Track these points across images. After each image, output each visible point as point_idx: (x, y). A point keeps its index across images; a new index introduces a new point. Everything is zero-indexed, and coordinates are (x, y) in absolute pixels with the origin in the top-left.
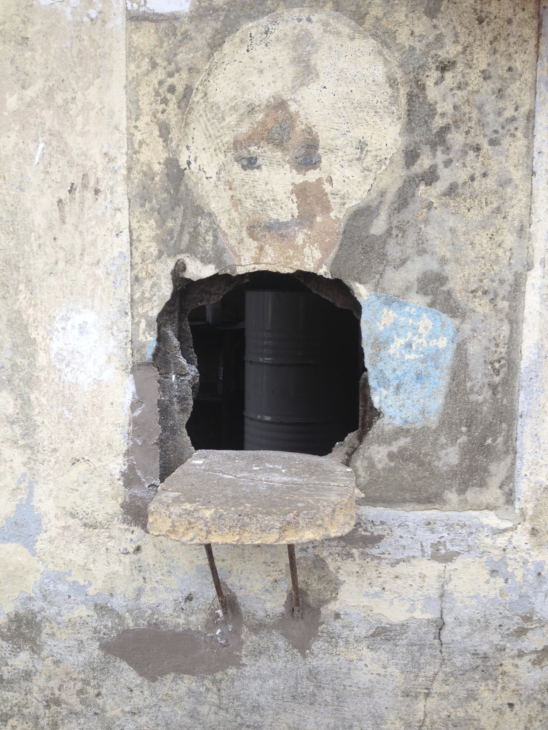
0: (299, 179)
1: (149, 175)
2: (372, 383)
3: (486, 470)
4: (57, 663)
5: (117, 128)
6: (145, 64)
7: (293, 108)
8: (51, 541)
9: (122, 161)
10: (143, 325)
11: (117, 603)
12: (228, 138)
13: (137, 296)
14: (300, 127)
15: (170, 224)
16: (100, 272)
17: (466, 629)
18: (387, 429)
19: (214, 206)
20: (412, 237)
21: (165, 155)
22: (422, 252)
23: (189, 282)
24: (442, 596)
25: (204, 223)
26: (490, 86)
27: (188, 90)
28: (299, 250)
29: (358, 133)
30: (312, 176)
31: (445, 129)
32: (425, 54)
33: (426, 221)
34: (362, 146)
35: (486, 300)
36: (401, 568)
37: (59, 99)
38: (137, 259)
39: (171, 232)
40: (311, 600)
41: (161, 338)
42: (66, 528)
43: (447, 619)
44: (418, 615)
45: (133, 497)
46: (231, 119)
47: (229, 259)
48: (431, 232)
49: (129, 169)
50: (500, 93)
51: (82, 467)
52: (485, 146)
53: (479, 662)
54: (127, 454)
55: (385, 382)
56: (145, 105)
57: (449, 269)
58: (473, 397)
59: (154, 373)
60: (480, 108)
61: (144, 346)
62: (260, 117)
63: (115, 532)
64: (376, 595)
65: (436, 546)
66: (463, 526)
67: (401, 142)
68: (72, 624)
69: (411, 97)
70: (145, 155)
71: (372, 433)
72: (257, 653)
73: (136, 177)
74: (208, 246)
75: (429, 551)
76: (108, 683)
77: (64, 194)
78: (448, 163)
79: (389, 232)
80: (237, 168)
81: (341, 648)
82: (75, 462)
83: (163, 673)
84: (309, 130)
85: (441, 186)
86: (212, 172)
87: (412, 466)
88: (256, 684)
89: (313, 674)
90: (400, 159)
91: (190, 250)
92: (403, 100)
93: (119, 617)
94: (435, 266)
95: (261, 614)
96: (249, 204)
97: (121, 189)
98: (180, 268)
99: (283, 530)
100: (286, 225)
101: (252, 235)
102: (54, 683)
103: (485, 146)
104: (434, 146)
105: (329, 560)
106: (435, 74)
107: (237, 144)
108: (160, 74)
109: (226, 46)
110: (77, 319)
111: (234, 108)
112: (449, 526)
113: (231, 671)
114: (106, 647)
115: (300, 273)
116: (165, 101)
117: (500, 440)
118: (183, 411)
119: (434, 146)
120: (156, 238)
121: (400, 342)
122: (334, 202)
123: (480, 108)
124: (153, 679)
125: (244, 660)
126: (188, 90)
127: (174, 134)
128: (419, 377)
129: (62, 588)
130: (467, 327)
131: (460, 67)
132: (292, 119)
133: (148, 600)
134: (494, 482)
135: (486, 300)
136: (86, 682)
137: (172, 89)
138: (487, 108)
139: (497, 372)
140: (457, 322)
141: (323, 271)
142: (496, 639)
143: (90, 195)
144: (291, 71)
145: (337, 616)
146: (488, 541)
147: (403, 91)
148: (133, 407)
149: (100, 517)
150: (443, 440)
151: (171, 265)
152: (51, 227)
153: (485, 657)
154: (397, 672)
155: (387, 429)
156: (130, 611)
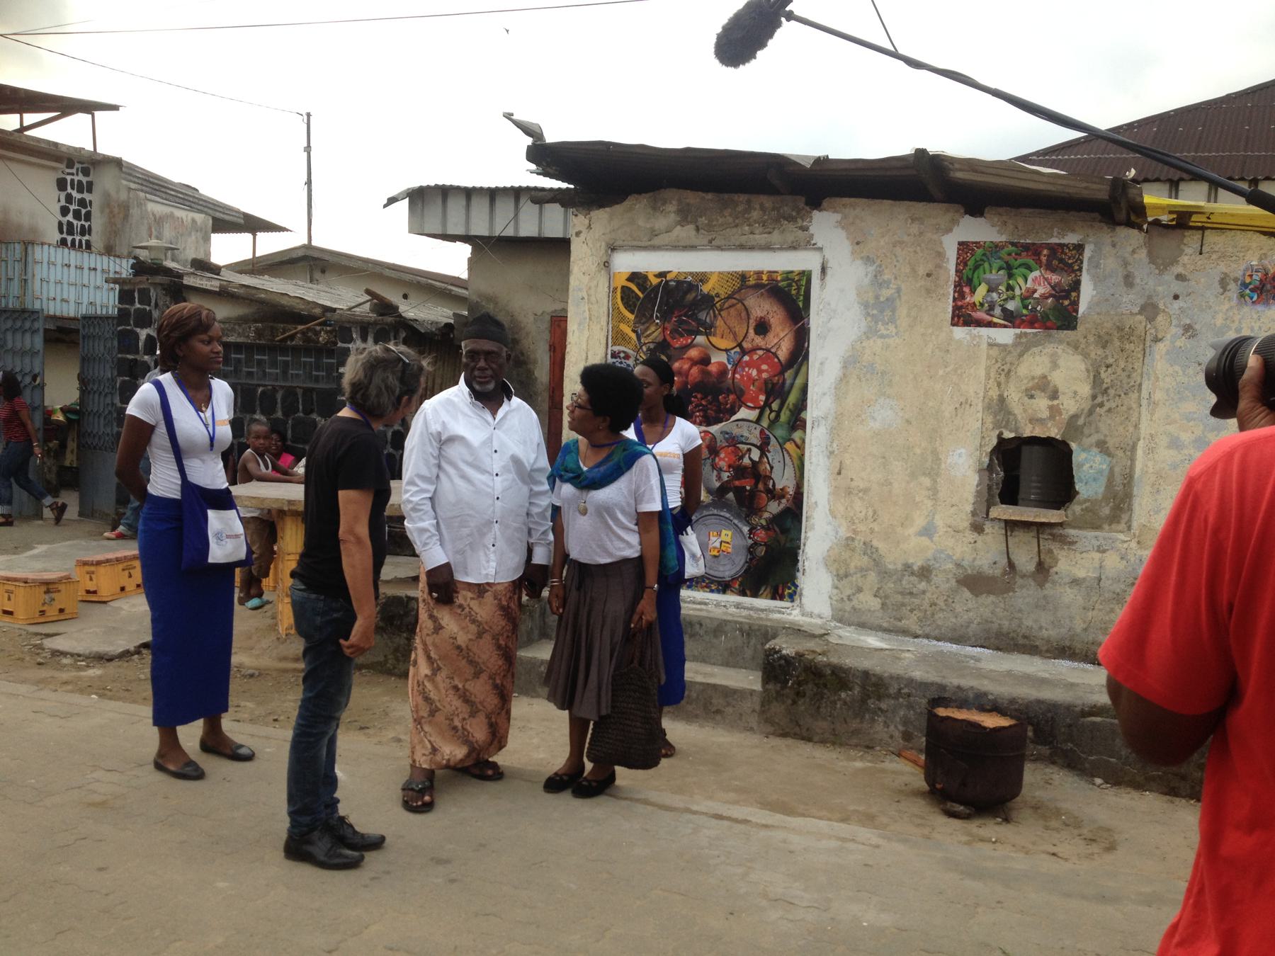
0: (1050, 403)
1: (992, 400)
2: (1076, 480)
3: (1120, 517)
4: (937, 587)
5: (980, 383)
6: (994, 361)
7: (1049, 378)
8: (940, 537)
9: (982, 394)
10: (984, 454)
11: (965, 563)
12: (1023, 388)
13: (983, 443)
14: (1051, 385)
15: (998, 417)
16: (969, 434)
17: (1110, 582)
18: (1081, 499)
19: (1016, 412)
20: (1093, 426)
21: (998, 393)
22: (1097, 432)
23: (1004, 439)
24: (1101, 567)
25: (1011, 417)
26: (1125, 374)
27: (1009, 371)
28: (1049, 429)
29: (1074, 388)
30: (1055, 402)
31: (1108, 388)
32: (1101, 361)
33: (1099, 421)
34: (1075, 393)
35: (1122, 451)
36: (1084, 555)
37: (959, 372)
38: (984, 430)
39: (998, 421)
40: (1046, 566)
41: (991, 460)
42: (946, 532)
43: (1103, 577)
44: (1090, 574)
45: (975, 521)
46: (1025, 381)
47: (1020, 431)
48: (1100, 425)
49: (984, 398)
50: (1129, 376)
51: (955, 508)
52: (1123, 395)
53: (1115, 596)
54: (973, 504)
55: (1081, 481)
56: (992, 375)
57: (1108, 439)
58: (1116, 488)
59: (987, 473)
60: (1121, 381)
61: (983, 462)
62: (1036, 381)
63: (966, 535)
64: (1073, 565)
65: (1099, 547)
66: (1110, 539)
67: (1090, 392)
68: (945, 571)
69: (1095, 376)
70: (991, 393)
71: (1074, 501)
72: (1022, 587)
73: (986, 400)
74: (1013, 426)
75: (1096, 549)
76: (958, 597)
77: (958, 406)
78: (1108, 400)
79: (1085, 424)
80: (1026, 398)
81: (1057, 587)
82: (953, 506)
83: (982, 594)
84: (1055, 386)
85: (1105, 408)
86: (1016, 400)
87: (1090, 514)
88: (1021, 600)
89: (1045, 597)
90: (1090, 398)
91: (1005, 427)
92: (1092, 377)
93: (965, 569)
94: (1102, 438)
95: (1024, 571)
96: (1030, 411)
97: (980, 404)
98: (1001, 433)
99: (1035, 517)
100: (1044, 419)
101: (1030, 423)
102: (935, 596)
103: (1123, 395)
104: (1103, 394)
105: (1055, 551)
106: (1104, 369)
107: (1027, 390)
108: (999, 365)
109: (1025, 356)
110: (959, 451)
111: (1027, 377)
112: (1104, 539)
113: (1011, 594)
114: (957, 581)
115: (1049, 438)
116: (1000, 374)
117: (1126, 505)
118: (998, 488)
119: (1103, 394)
120: (992, 422)
121: (1088, 465)
122: (1064, 412)
123: (1121, 381)
124: (977, 596)
125: (1016, 590)
126: (1009, 371)
127: (1003, 386)
128: (1095, 480)
129: (943, 556)
130: (1114, 461)
131: (1114, 366)
132: (1049, 382)
133: (978, 563)
134: (1123, 521)
135: (1122, 451)
136: (948, 596)
137: (1003, 370)
138: (1124, 382)
139: (1126, 479)
140: (1110, 459)
141: (1058, 437)
142: (1123, 586)
143: (968, 406)
144: (1049, 365)
145: (1057, 573)
146: (1120, 545)
147: (1092, 374)
148: (977, 486)
149: (961, 528)
150: (1103, 504)
151: (997, 432)
152: (952, 417)
153: (1118, 594)
154: (1081, 599)
155: (1081, 499)
156: (970, 567)
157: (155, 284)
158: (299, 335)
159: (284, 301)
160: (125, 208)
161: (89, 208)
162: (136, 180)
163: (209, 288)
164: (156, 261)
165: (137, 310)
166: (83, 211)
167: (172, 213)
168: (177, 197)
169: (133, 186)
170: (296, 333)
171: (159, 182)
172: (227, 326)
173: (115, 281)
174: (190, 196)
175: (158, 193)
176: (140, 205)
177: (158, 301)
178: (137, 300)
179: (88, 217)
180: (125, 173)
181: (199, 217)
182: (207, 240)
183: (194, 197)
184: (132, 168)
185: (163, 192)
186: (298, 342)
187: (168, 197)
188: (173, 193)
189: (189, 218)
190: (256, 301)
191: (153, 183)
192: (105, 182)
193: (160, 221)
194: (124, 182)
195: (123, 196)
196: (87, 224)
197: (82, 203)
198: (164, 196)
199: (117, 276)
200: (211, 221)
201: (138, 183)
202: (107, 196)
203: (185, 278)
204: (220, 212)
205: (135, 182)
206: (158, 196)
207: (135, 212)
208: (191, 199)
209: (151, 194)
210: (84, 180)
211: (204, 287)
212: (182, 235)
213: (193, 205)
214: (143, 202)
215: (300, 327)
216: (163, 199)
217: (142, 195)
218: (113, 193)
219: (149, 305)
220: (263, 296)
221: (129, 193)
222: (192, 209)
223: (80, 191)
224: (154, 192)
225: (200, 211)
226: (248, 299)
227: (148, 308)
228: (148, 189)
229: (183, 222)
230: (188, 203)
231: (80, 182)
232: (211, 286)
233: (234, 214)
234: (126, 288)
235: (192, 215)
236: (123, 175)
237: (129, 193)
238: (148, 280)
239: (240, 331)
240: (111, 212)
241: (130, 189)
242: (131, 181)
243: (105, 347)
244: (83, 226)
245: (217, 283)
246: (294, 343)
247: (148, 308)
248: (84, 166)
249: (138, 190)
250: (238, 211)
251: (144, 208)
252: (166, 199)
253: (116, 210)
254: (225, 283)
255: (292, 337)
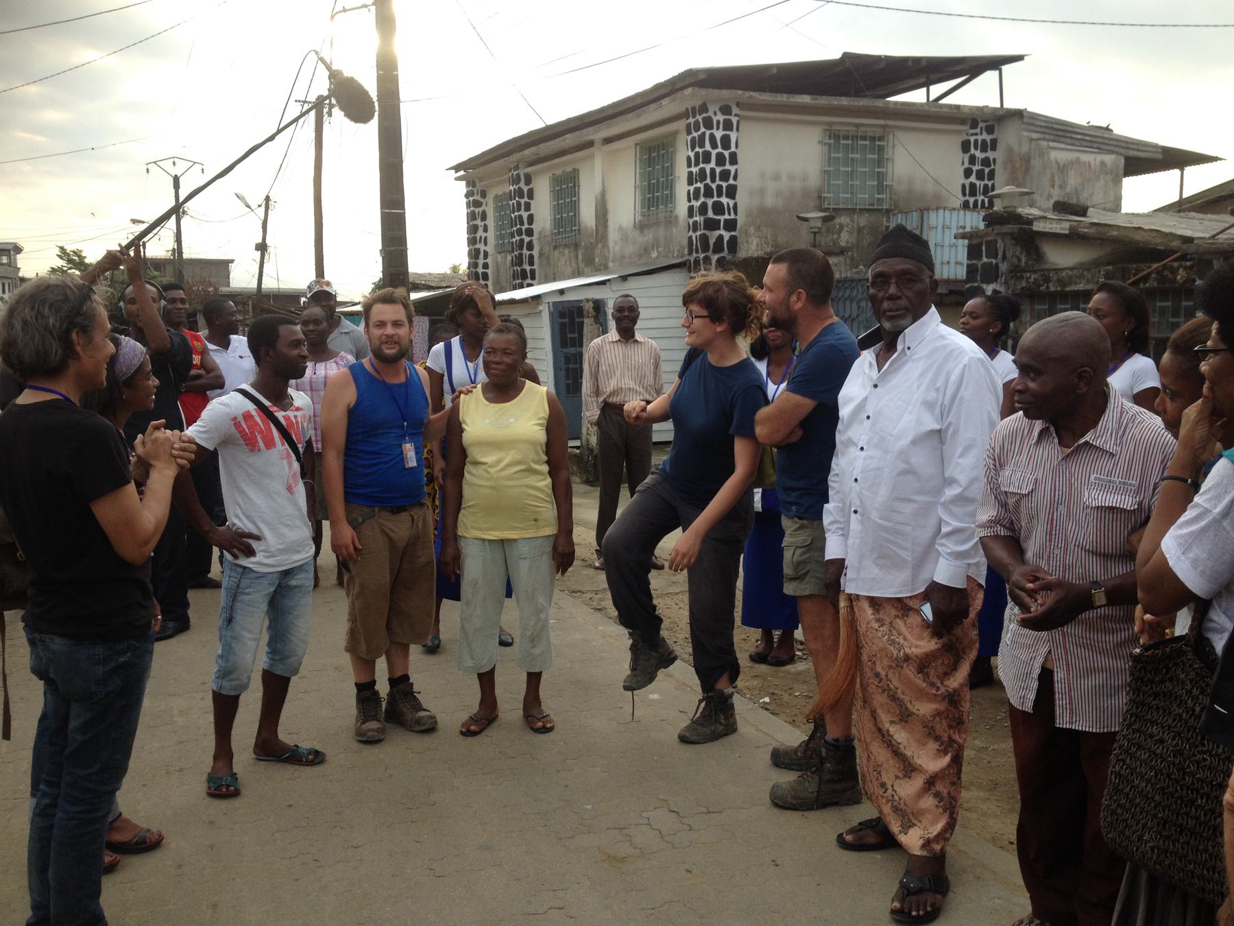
157: (1003, 235)
158: (1153, 276)
159: (1139, 237)
160: (1027, 160)
161: (993, 167)
162: (1038, 129)
163: (1058, 231)
164: (1009, 210)
165: (985, 263)
166: (987, 170)
167: (1078, 160)
168: (1083, 140)
169: (1035, 136)
170: (1149, 274)
171: (1064, 128)
172: (1076, 272)
173: (963, 236)
174: (1100, 137)
175: (1063, 139)
176: (1042, 155)
177: (1007, 253)
178: (984, 254)
179: (992, 175)
180: (1026, 124)
181: (1109, 159)
182: (1117, 183)
183: (1103, 138)
184: (1034, 117)
185: (1067, 137)
186: (1152, 283)
187: (1074, 142)
188: (1079, 137)
189: (1098, 162)
190: (1108, 240)
191: (1056, 130)
192: (1010, 137)
193: (1063, 169)
194: (1025, 134)
195: (1025, 148)
196: (990, 184)
197: (986, 162)
198: (1069, 141)
199: (961, 231)
200: (1123, 161)
201: (1040, 132)
202: (1010, 150)
203: (1034, 223)
204: (1134, 149)
205: (1037, 132)
206: (1063, 143)
207: (1036, 163)
208: (1100, 140)
209: (1054, 141)
210: (988, 138)
211: (1054, 231)
212: (1088, 182)
213: (1102, 146)
214: (1044, 151)
215: (1155, 266)
216: (1067, 144)
217: (1044, 143)
218: (1015, 147)
219: (996, 258)
220: (1115, 233)
221: (1030, 144)
222: (1101, 151)
223: (984, 150)
224: (1057, 138)
225: (1111, 152)
226: (1097, 239)
227: (994, 261)
228: (1052, 137)
229: (1090, 166)
230: (1095, 145)
231: (984, 142)
232: (1061, 229)
233: (1150, 149)
234: (975, 242)
235: (1100, 157)
236: (1023, 126)
237: (1030, 144)
238: (993, 230)
239: (1089, 276)
240: (1013, 167)
241: (1031, 140)
242: (1033, 131)
243: (859, 307)
244: (986, 186)
245: (1066, 225)
246: (1148, 285)
247: (994, 261)
248: (988, 124)
249: (1040, 139)
250: (1156, 146)
251: (1046, 158)
252: (1073, 145)
253: (1018, 165)
254: (1075, 224)
255: (1145, 279)
